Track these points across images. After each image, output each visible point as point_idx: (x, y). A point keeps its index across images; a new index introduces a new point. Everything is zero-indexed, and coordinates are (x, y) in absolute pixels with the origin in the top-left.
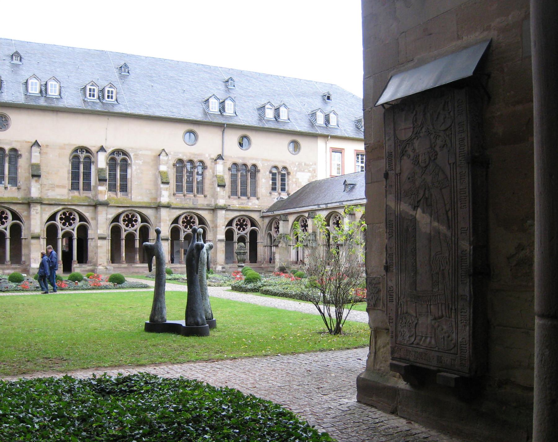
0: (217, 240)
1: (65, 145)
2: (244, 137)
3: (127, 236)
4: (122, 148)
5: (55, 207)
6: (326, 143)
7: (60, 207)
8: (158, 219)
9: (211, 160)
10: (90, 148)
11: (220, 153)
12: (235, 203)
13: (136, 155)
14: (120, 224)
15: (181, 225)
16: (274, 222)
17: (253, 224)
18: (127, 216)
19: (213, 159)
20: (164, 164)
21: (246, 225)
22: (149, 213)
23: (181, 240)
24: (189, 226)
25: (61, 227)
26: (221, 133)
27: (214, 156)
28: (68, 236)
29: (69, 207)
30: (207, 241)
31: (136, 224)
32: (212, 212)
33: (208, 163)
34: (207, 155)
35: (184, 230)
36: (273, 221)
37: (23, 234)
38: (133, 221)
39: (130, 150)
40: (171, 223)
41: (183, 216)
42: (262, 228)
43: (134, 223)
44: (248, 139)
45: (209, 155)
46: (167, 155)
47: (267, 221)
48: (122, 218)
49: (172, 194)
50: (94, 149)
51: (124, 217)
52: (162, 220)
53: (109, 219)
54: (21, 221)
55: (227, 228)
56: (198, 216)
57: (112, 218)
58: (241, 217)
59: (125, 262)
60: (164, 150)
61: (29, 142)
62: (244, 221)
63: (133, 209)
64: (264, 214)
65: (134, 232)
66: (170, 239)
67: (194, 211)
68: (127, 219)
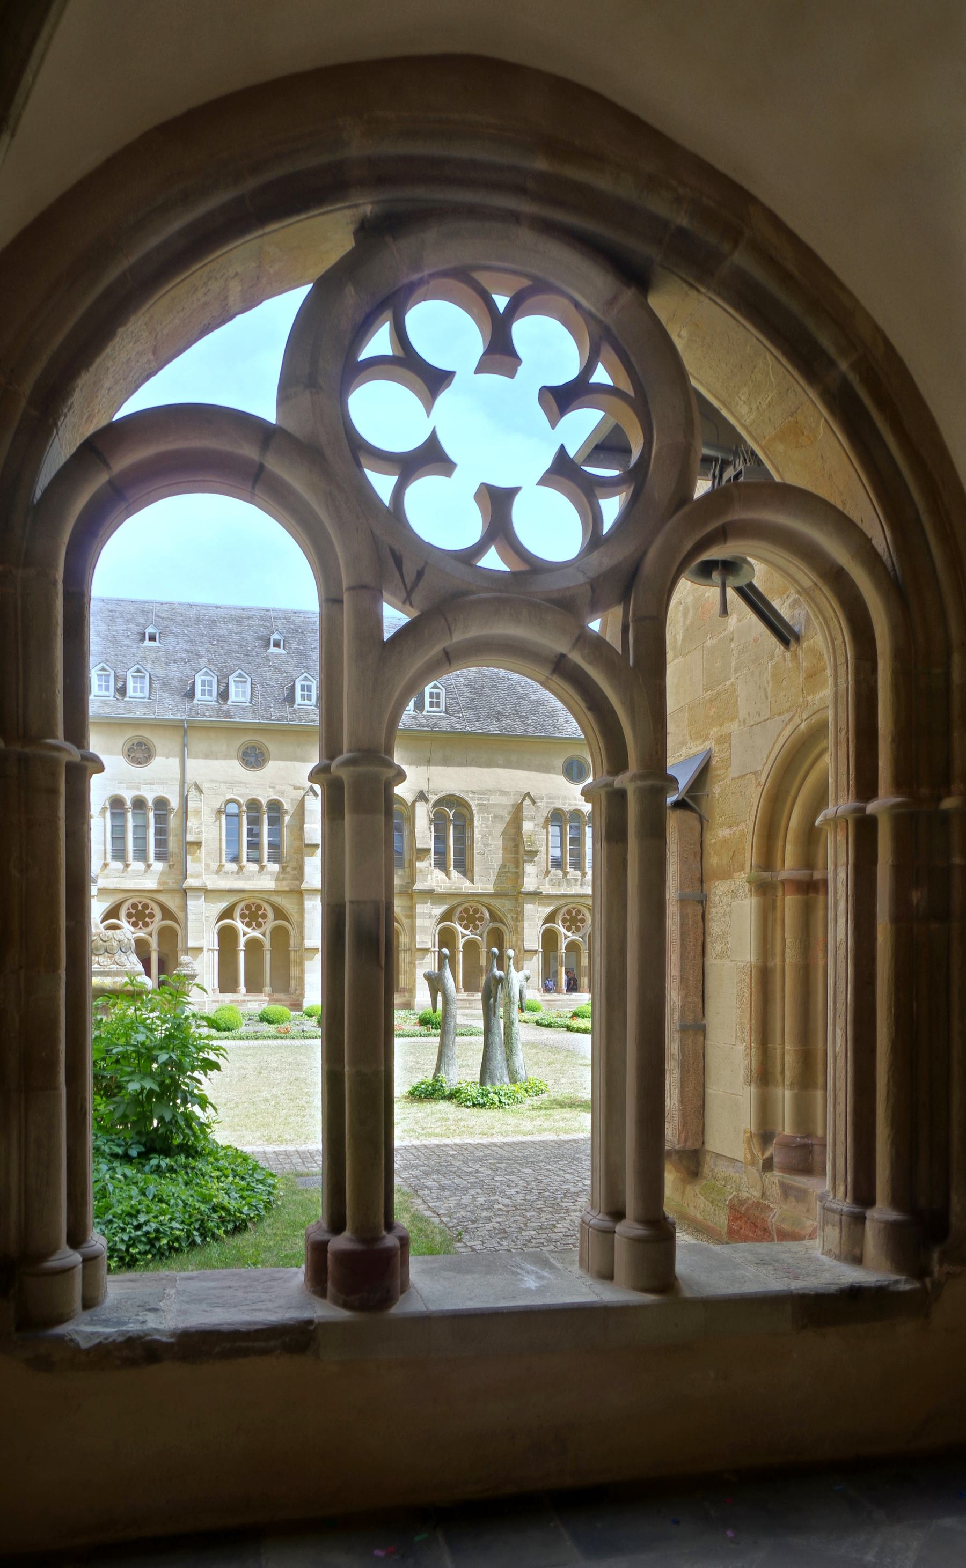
3: (465, 946)
4: (457, 793)
8: (519, 916)
37: (292, 942)
38: (476, 919)
40: (541, 922)
51: (461, 913)
60: (529, 793)
61: (299, 788)
66: (541, 950)
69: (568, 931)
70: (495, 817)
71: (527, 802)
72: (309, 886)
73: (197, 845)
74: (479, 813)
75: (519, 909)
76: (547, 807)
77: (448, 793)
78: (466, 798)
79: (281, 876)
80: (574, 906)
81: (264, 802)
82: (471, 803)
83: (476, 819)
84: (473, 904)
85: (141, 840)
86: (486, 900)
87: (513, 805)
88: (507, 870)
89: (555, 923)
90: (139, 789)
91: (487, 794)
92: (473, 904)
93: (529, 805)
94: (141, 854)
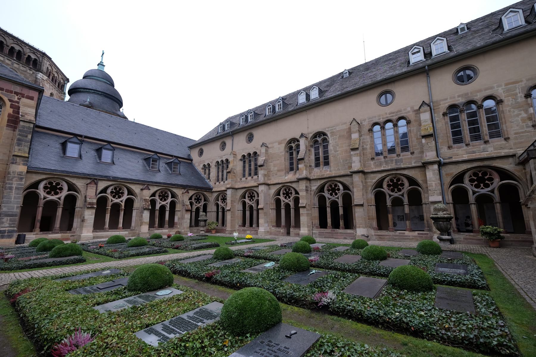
1: (282, 140)
4: (320, 130)
5: (278, 185)
7: (281, 186)
13: (333, 133)
20: (355, 132)
28: (287, 206)
29: (286, 184)
31: (339, 193)
33: (411, 116)
34: (409, 109)
38: (336, 190)
39: (327, 129)
43: (337, 191)
44: (472, 69)
45: (412, 108)
48: (326, 188)
49: (370, 159)
50: (298, 137)
53: (314, 190)
57: (317, 189)
63: (333, 179)
74: (331, 137)
76: (369, 124)
80: (394, 176)
81: (252, 153)
84: (333, 182)
88: (348, 162)
90: (222, 158)
92: (333, 182)
93: (355, 125)
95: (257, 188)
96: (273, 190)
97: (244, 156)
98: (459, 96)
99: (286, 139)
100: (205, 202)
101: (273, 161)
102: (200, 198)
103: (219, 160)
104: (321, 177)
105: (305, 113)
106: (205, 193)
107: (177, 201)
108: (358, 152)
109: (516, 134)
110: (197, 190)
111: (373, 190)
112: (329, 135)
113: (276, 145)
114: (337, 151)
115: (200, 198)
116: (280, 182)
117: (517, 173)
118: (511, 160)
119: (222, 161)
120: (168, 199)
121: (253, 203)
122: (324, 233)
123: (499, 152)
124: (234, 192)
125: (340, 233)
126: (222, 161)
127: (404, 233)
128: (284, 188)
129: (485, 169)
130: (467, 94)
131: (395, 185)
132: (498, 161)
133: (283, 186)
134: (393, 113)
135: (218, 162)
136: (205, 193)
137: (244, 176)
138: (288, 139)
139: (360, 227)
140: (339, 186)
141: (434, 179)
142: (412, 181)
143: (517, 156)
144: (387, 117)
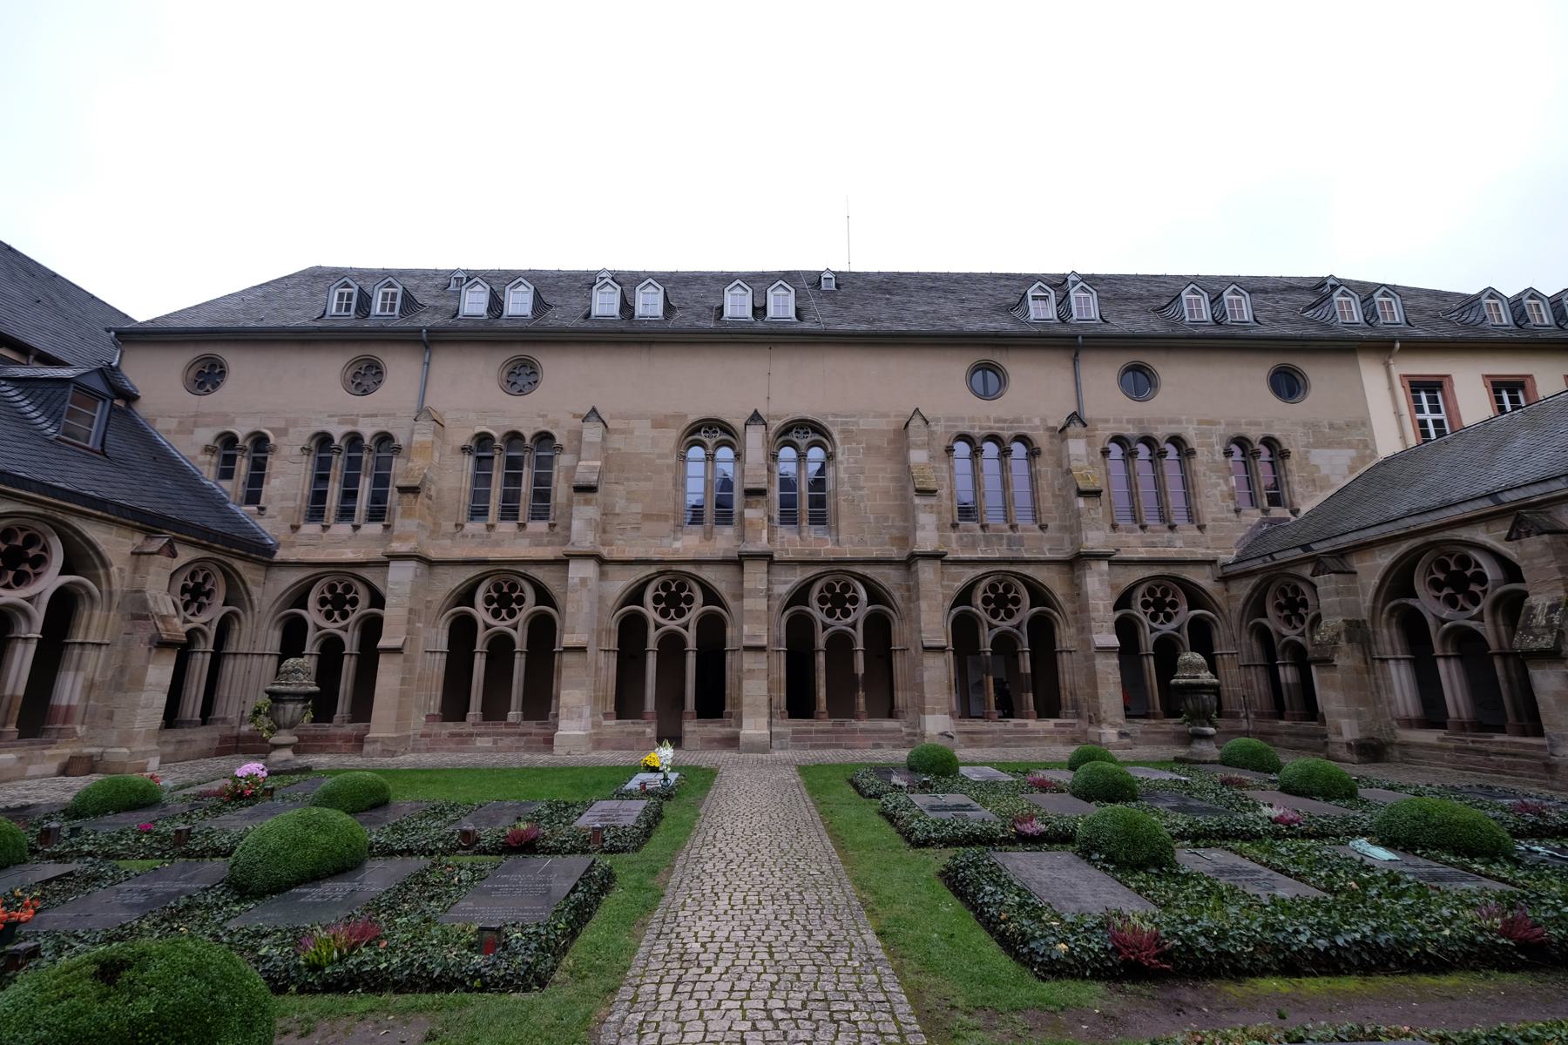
0: (1093, 650)
1: (666, 416)
2: (1137, 369)
3: (829, 643)
4: (810, 417)
6: (1387, 367)
7: (653, 569)
8: (913, 592)
9: (1048, 433)
10: (728, 420)
11: (1072, 409)
12: (1135, 545)
13: (846, 433)
14: (808, 609)
15: (981, 608)
16: (1273, 588)
17: (1196, 597)
18: (830, 587)
19: (1054, 429)
20: (920, 447)
21: (1174, 605)
22: (888, 578)
23: (984, 652)
24: (1002, 611)
25: (655, 620)
26: (1070, 364)
27: (1058, 421)
29: (674, 568)
30: (1061, 652)
32: (1066, 569)
33: (1041, 439)
34: (1037, 421)
35: (989, 623)
36: (1269, 585)
39: (830, 419)
40: (948, 604)
41: (985, 583)
42: (1227, 611)
44: (1147, 373)
45: (1044, 420)
46: (927, 423)
47: (1243, 589)
48: (815, 593)
49: (949, 525)
51: (821, 591)
52: (922, 594)
53: (780, 595)
54: (554, 606)
55: (1118, 614)
56: (1025, 583)
57: (789, 593)
58: (1157, 582)
59: (826, 715)
62: (1165, 593)
63: (844, 568)
64: (1226, 569)
65: (849, 629)
66: (951, 648)
67: (1014, 568)
68: (829, 595)
69: (995, 618)
70: (868, 448)
71: (917, 421)
72: (575, 549)
73: (413, 492)
74: (843, 443)
75: (912, 583)
76: (946, 432)
77: (797, 416)
78: (824, 424)
79: (546, 540)
80: (1000, 577)
81: (528, 434)
82: (830, 428)
83: (839, 451)
84: (839, 577)
85: (349, 495)
86: (859, 569)
87: (894, 430)
88: (890, 524)
89: (971, 606)
90: (355, 423)
91: (854, 416)
92: (839, 577)
93: (919, 427)
94: (346, 514)
95: (384, 569)
96: (620, 583)
97: (483, 440)
98: (1129, 421)
99: (686, 416)
100: (227, 609)
101: (627, 479)
102: (208, 587)
103: (338, 432)
104: (809, 558)
105: (766, 349)
106: (239, 565)
107: (95, 590)
108: (932, 501)
109: (1214, 520)
110: (205, 547)
111: (951, 609)
112: (836, 436)
113: (643, 428)
114: (861, 488)
115: (208, 587)
116: (656, 557)
117: (1218, 598)
118: (1208, 569)
119: (354, 439)
120: (37, 575)
121: (345, 629)
122: (811, 732)
123: (1192, 552)
124: (422, 574)
125: (862, 731)
126: (354, 439)
127: (1026, 725)
128: (494, 579)
129: (1167, 583)
130: (1141, 421)
131: (1001, 602)
132: (1190, 568)
133: (660, 574)
134: (1005, 421)
135: (324, 440)
136: (239, 565)
137: (478, 512)
138: (692, 418)
139: (933, 712)
140: (855, 591)
141: (1101, 595)
142: (1039, 594)
143: (1220, 562)
144: (990, 428)
